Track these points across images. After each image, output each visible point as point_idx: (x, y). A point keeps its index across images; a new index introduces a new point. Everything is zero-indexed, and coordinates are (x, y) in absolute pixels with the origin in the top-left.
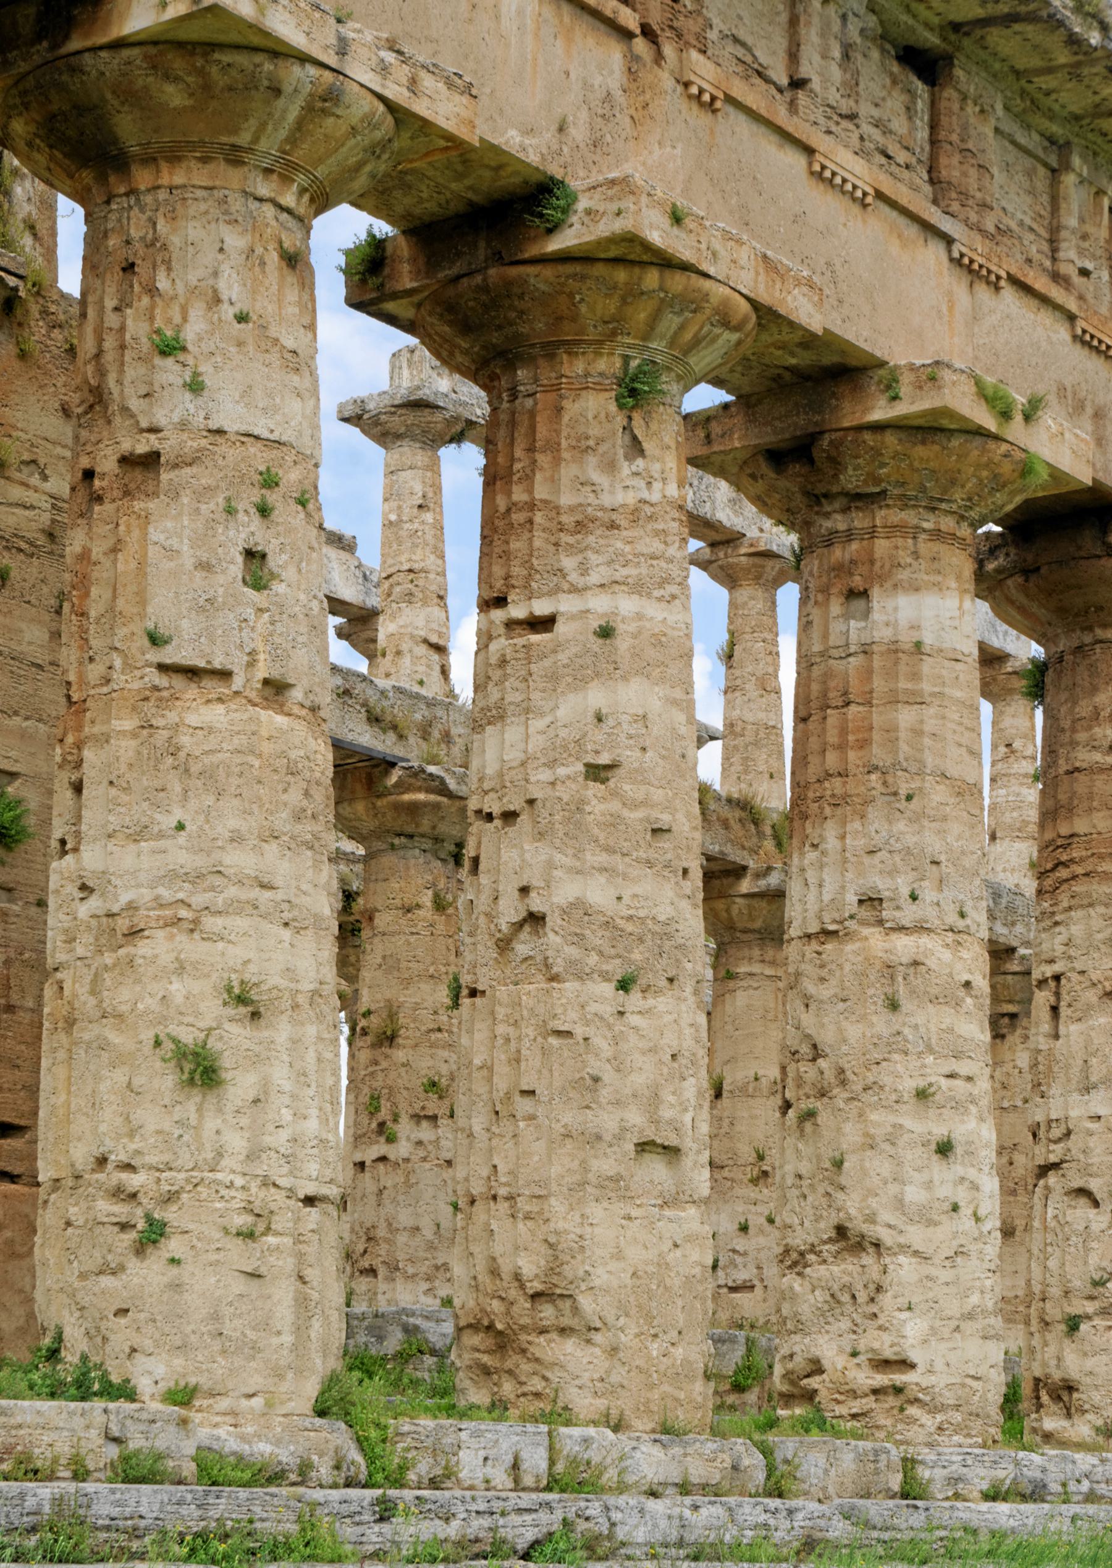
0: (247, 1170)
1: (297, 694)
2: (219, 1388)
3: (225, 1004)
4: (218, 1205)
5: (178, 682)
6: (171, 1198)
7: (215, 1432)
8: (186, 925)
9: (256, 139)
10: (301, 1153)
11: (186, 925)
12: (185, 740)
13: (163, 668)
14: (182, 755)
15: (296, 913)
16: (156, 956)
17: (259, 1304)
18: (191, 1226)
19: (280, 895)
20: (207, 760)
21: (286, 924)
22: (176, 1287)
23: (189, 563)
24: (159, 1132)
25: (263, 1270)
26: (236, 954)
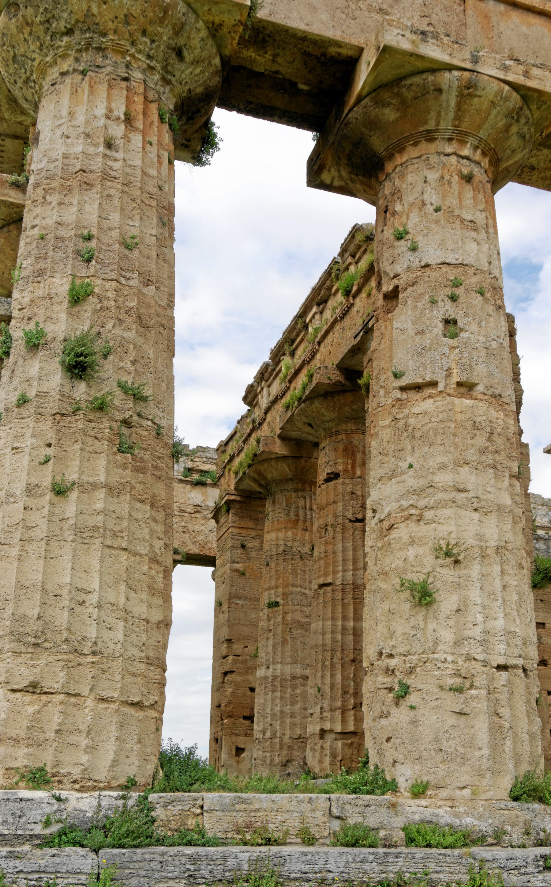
0: (455, 651)
1: (480, 388)
2: (441, 783)
3: (437, 558)
4: (436, 673)
5: (412, 395)
6: (411, 671)
7: (437, 811)
8: (415, 518)
9: (438, 123)
10: (493, 640)
11: (415, 518)
12: (412, 421)
13: (403, 389)
14: (410, 429)
15: (484, 503)
16: (401, 538)
17: (466, 731)
18: (422, 687)
19: (471, 494)
20: (424, 429)
21: (476, 510)
22: (414, 722)
23: (411, 332)
24: (404, 634)
25: (466, 710)
26: (444, 529)
